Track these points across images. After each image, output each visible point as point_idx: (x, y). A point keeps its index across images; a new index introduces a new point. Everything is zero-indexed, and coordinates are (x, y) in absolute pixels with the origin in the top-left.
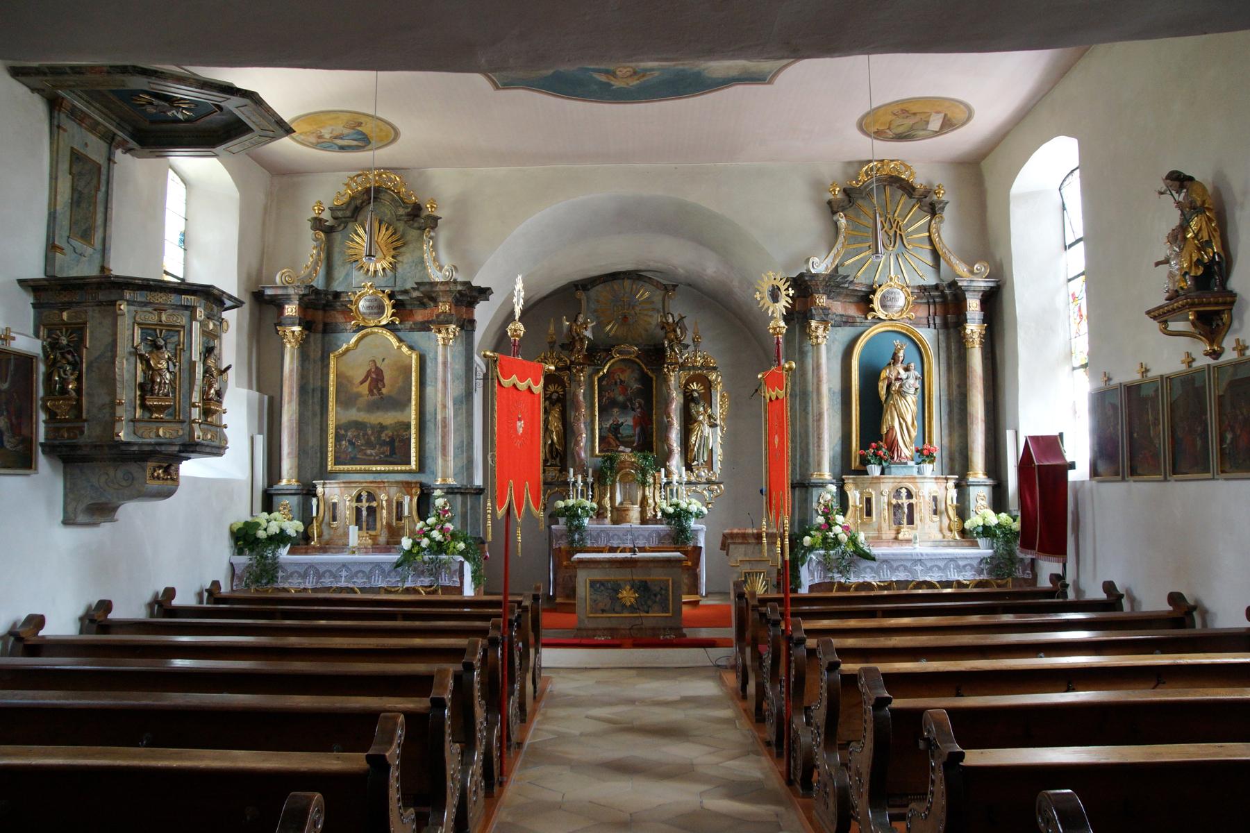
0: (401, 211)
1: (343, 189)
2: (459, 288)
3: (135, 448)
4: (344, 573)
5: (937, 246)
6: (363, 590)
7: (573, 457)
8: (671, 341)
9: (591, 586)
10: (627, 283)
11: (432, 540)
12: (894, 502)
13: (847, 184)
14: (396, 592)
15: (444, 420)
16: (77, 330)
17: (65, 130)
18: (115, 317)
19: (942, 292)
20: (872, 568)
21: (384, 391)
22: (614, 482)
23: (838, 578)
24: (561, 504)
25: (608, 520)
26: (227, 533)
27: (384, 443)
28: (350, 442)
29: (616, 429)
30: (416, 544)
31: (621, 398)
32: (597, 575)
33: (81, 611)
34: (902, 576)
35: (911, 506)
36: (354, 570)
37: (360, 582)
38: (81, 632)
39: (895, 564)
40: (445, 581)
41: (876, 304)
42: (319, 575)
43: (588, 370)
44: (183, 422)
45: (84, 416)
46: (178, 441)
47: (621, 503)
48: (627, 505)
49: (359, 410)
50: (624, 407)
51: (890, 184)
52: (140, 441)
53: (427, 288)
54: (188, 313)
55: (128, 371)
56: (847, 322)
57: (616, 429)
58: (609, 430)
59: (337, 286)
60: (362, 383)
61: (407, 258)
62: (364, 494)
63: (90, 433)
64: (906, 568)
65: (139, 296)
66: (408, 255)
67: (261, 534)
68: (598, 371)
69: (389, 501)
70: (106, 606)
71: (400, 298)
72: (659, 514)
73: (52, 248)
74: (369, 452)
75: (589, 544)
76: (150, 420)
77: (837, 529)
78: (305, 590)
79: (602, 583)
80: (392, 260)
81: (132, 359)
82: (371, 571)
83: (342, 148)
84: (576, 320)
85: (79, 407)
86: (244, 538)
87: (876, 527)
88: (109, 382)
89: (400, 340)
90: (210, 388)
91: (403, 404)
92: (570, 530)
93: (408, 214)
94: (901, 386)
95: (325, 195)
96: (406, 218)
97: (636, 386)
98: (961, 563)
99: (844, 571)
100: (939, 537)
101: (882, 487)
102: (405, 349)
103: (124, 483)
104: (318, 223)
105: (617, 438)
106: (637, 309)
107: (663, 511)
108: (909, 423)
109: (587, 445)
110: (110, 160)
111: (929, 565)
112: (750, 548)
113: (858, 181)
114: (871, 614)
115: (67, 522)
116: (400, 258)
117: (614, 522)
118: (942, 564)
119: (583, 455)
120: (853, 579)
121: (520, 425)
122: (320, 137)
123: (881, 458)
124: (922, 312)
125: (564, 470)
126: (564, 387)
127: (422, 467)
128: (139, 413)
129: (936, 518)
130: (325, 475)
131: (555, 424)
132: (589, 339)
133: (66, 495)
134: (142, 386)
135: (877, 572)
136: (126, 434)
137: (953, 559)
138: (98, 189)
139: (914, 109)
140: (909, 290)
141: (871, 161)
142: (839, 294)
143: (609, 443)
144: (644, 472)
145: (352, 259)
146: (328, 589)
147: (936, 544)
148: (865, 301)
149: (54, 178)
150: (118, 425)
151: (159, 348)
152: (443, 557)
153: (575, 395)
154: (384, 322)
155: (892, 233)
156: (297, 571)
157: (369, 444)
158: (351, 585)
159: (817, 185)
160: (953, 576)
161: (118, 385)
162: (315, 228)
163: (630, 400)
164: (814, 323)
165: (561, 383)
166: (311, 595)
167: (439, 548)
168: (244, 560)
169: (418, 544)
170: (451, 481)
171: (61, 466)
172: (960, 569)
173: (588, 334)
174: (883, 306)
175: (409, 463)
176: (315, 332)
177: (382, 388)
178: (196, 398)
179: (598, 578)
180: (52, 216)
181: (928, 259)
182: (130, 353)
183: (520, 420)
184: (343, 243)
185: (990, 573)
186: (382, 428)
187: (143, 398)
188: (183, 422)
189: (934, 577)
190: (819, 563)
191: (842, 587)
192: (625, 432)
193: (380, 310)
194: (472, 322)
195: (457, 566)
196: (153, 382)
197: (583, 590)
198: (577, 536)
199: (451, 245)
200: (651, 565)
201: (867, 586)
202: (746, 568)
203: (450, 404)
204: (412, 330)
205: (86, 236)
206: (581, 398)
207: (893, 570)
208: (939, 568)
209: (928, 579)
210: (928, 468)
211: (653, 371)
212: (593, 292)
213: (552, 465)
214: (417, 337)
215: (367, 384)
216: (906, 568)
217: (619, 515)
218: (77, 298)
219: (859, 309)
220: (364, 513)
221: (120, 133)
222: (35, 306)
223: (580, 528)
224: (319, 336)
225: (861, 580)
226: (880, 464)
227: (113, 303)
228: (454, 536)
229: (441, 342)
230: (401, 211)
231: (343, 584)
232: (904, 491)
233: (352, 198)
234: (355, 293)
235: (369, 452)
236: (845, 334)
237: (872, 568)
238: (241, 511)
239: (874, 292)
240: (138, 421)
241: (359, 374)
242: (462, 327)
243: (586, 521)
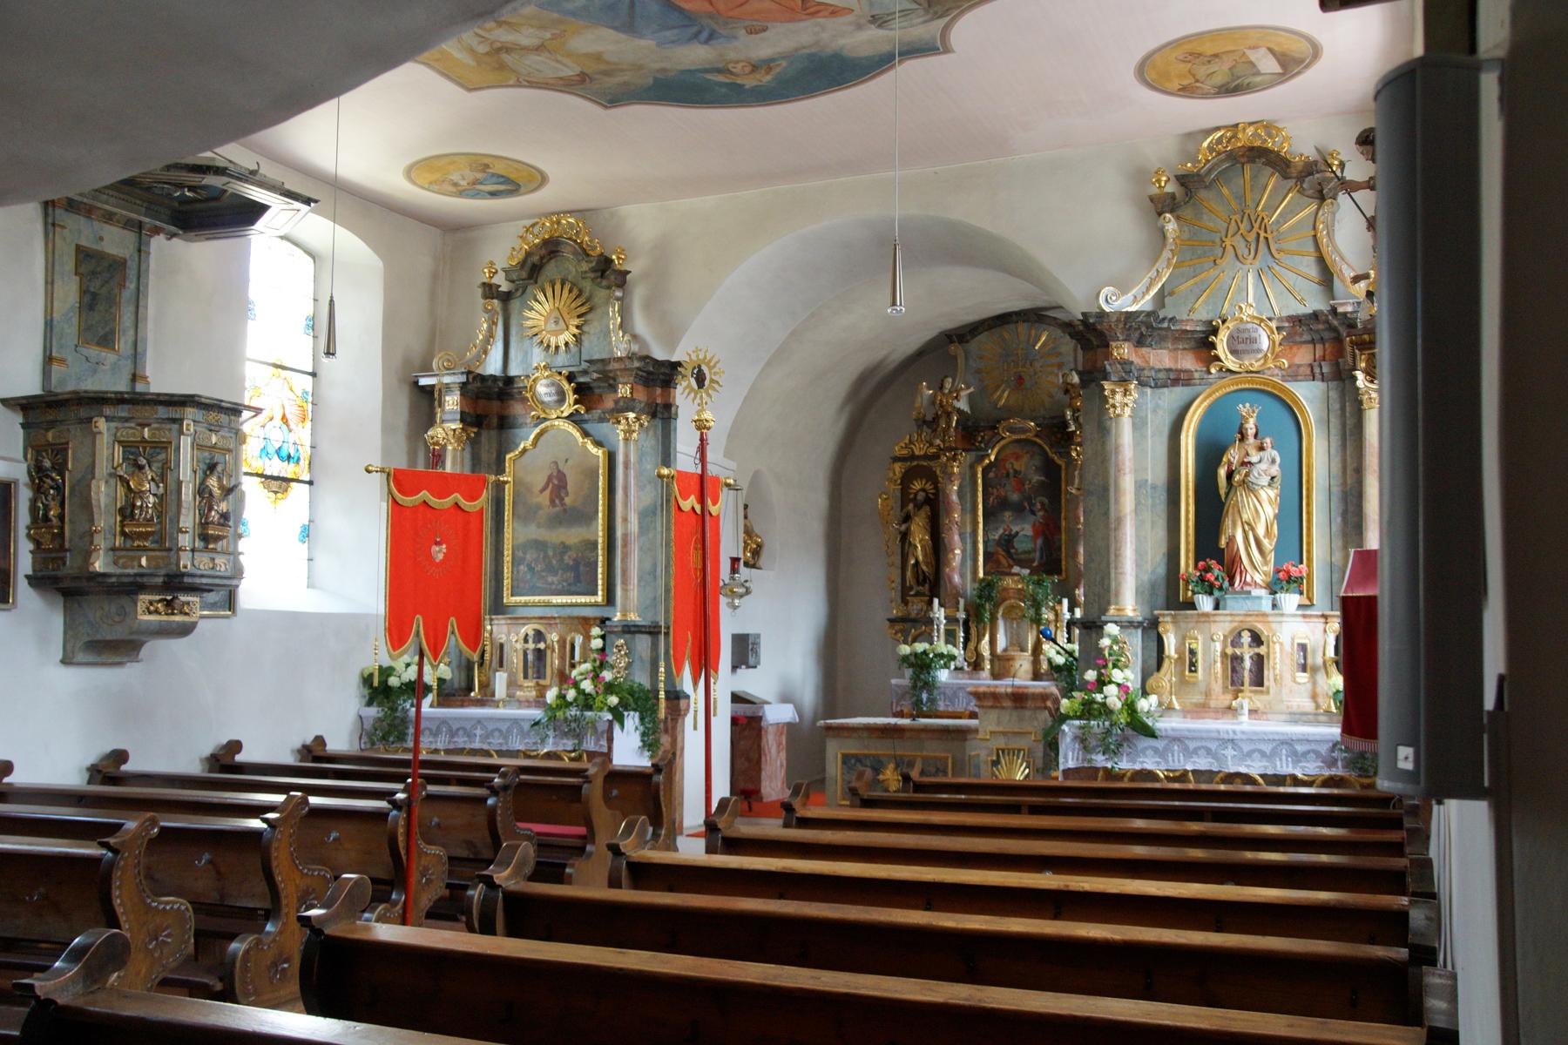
0: (585, 267)
1: (517, 243)
2: (637, 364)
3: (114, 580)
4: (478, 732)
5: (1324, 250)
6: (448, 752)
8: (1075, 410)
9: (844, 763)
10: (1022, 328)
11: (581, 692)
12: (1229, 651)
13: (1181, 171)
14: (535, 757)
15: (625, 536)
16: (60, 451)
17: (63, 227)
18: (94, 435)
19: (1327, 322)
20: (1156, 750)
21: (567, 500)
22: (993, 620)
23: (1100, 760)
24: (905, 649)
25: (986, 673)
26: (354, 681)
27: (567, 568)
28: (531, 569)
29: (1008, 541)
30: (562, 697)
31: (1015, 497)
32: (853, 747)
33: (91, 759)
34: (1203, 763)
35: (1259, 661)
36: (491, 727)
37: (496, 743)
38: (89, 782)
39: (1192, 745)
40: (590, 744)
41: (1222, 349)
42: (453, 734)
43: (966, 458)
44: (170, 550)
45: (67, 545)
46: (163, 572)
47: (1005, 650)
48: (1014, 653)
49: (539, 526)
50: (1019, 510)
51: (1252, 160)
52: (119, 571)
53: (599, 366)
54: (175, 427)
55: (104, 494)
56: (1177, 379)
57: (1008, 541)
58: (998, 543)
59: (513, 372)
60: (542, 491)
61: (593, 328)
62: (531, 633)
63: (71, 563)
64: (1209, 751)
65: (123, 411)
66: (596, 323)
67: (393, 681)
69: (562, 642)
70: (120, 756)
71: (582, 380)
72: (1045, 666)
73: (48, 360)
74: (550, 579)
75: (941, 707)
76: (132, 549)
77: (1111, 690)
78: (436, 751)
79: (858, 759)
80: (576, 331)
81: (112, 481)
82: (509, 730)
83: (493, 194)
84: (942, 387)
85: (62, 534)
86: (379, 689)
87: (1202, 687)
88: (87, 506)
89: (586, 434)
90: (211, 509)
91: (588, 517)
92: (914, 687)
93: (593, 270)
94: (1247, 475)
95: (500, 254)
96: (592, 275)
97: (1037, 478)
98: (1300, 748)
99: (1112, 751)
100: (1308, 706)
101: (1214, 628)
102: (590, 446)
103: (117, 619)
104: (490, 291)
105: (1008, 552)
106: (1037, 365)
107: (1050, 661)
108: (1261, 531)
109: (964, 564)
110: (141, 250)
111: (1246, 748)
112: (1006, 716)
113: (1195, 161)
114: (1014, 809)
115: (66, 661)
116: (585, 328)
117: (995, 676)
118: (1267, 748)
119: (957, 579)
120: (1124, 764)
121: (439, 552)
122: (455, 185)
123: (1212, 586)
124: (1304, 356)
126: (936, 483)
127: (610, 599)
128: (119, 541)
129: (1303, 677)
130: (498, 608)
131: (919, 537)
132: (959, 411)
133: (65, 633)
134: (121, 511)
135: (1162, 754)
136: (106, 565)
137: (1288, 742)
138: (122, 286)
139: (1209, 49)
140: (1273, 325)
141: (1218, 129)
142: (1163, 339)
143: (998, 563)
144: (1037, 605)
145: (530, 333)
146: (460, 751)
147: (1297, 717)
148: (1204, 344)
149: (50, 283)
150: (94, 555)
151: (141, 468)
152: (588, 714)
153: (947, 496)
154: (566, 414)
155: (1252, 237)
156: (442, 729)
157: (550, 569)
158: (485, 747)
159: (1140, 175)
160: (1285, 767)
161: (95, 510)
162: (485, 297)
163: (1029, 499)
164: (1107, 385)
165: (931, 476)
166: (442, 757)
167: (586, 701)
168: (373, 712)
169: (564, 697)
170: (633, 617)
171: (60, 600)
172: (1297, 757)
173: (963, 405)
174: (1234, 352)
175: (595, 593)
176: (489, 427)
177: (566, 499)
178: (188, 520)
179: (853, 751)
180: (49, 325)
181: (1313, 271)
182: (111, 475)
183: (437, 544)
184: (520, 313)
185: (1349, 764)
186: (565, 548)
187: (123, 526)
188: (170, 550)
189: (1254, 768)
190: (1076, 738)
191: (1109, 774)
192: (1021, 545)
193: (561, 398)
194: (668, 406)
195: (606, 726)
196: (134, 506)
197: (834, 768)
198: (924, 696)
199: (649, 306)
200: (923, 735)
201: (1150, 775)
202: (1001, 742)
203: (634, 519)
204: (602, 420)
205: (106, 341)
206: (954, 498)
207: (1189, 753)
208: (1263, 754)
209: (1243, 770)
210: (1290, 601)
211: (1061, 455)
212: (974, 345)
213: (917, 594)
214: (602, 429)
215: (548, 492)
216: (1209, 751)
217: (1002, 666)
218: (61, 416)
219: (1199, 359)
220: (530, 657)
221: (147, 220)
222: (23, 426)
223: (930, 686)
224: (494, 433)
225: (1138, 767)
226: (1211, 594)
227: (89, 420)
228: (610, 688)
229: (622, 435)
230: (585, 267)
231: (477, 745)
232: (1246, 638)
233: (528, 254)
234: (528, 377)
235: (550, 579)
236: (1171, 398)
237: (1156, 750)
238: (375, 653)
239: (1215, 331)
240: (120, 549)
241: (539, 480)
242: (654, 415)
243: (943, 676)
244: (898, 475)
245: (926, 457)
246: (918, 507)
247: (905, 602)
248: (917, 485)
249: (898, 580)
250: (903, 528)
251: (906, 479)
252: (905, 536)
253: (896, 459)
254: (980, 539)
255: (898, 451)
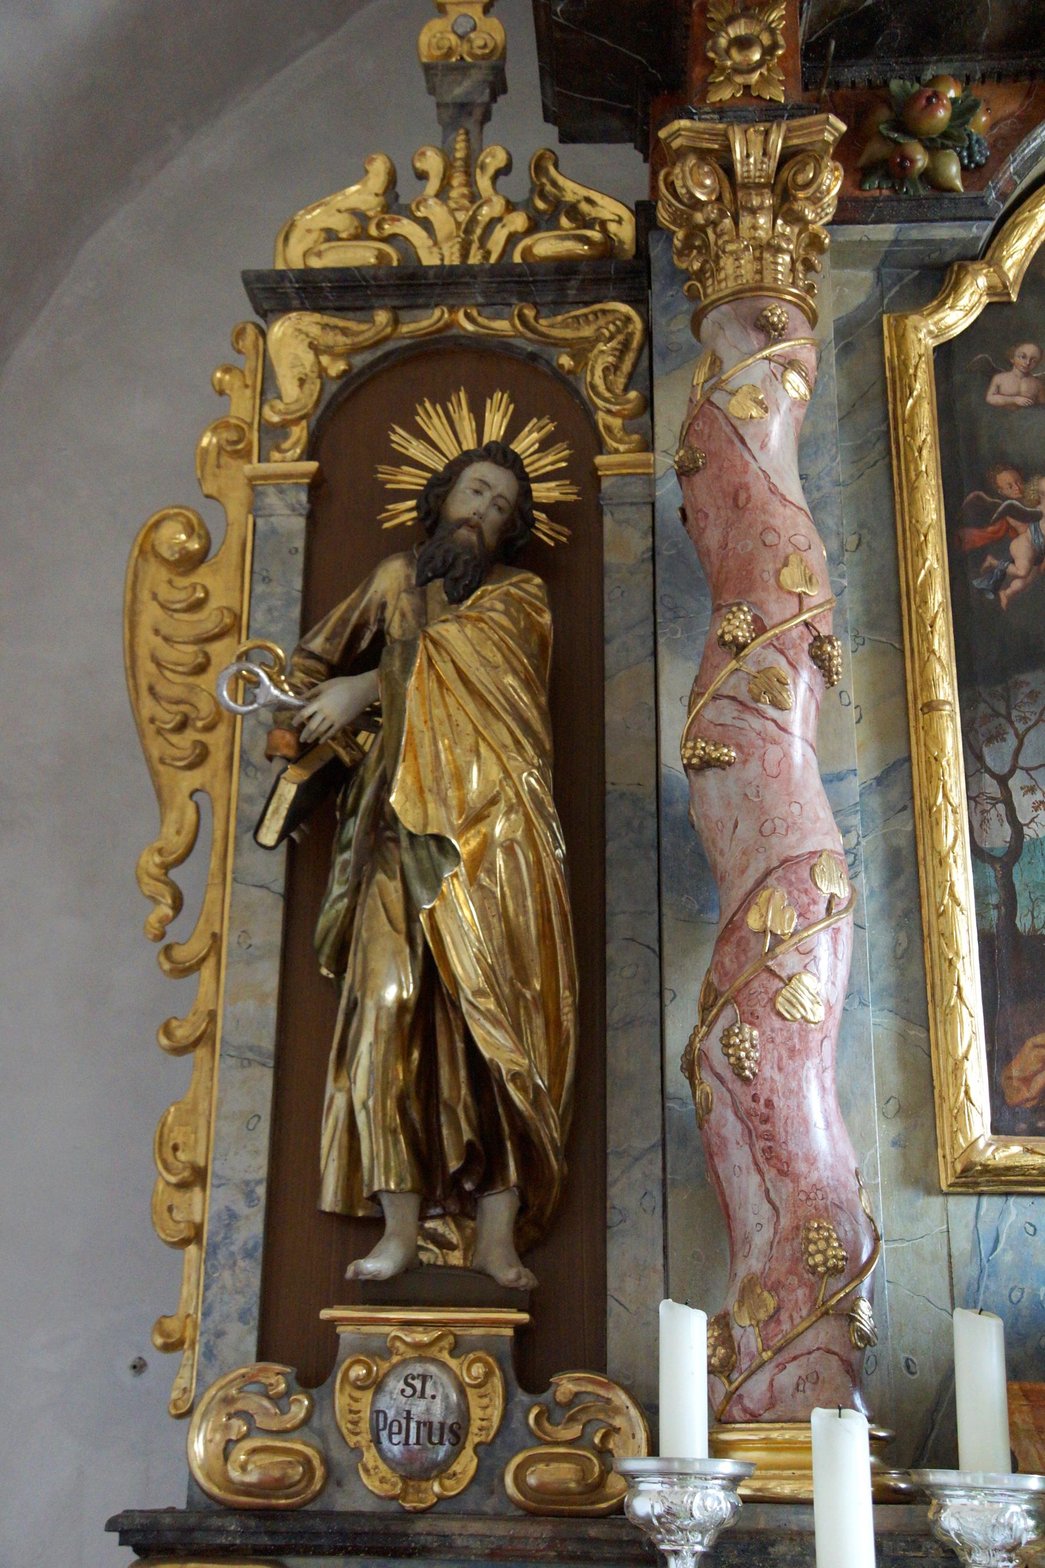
7: (689, 1155)
68: (936, 279)
125: (564, 1337)
126: (580, 434)
131: (465, 769)
153: (713, 446)
165: (545, 389)
244: (294, 393)
245: (515, 282)
246: (452, 569)
247: (296, 1344)
248: (441, 434)
249: (250, 1161)
250: (334, 702)
251: (351, 419)
252: (334, 806)
253: (278, 293)
254: (954, 835)
255: (319, 233)
